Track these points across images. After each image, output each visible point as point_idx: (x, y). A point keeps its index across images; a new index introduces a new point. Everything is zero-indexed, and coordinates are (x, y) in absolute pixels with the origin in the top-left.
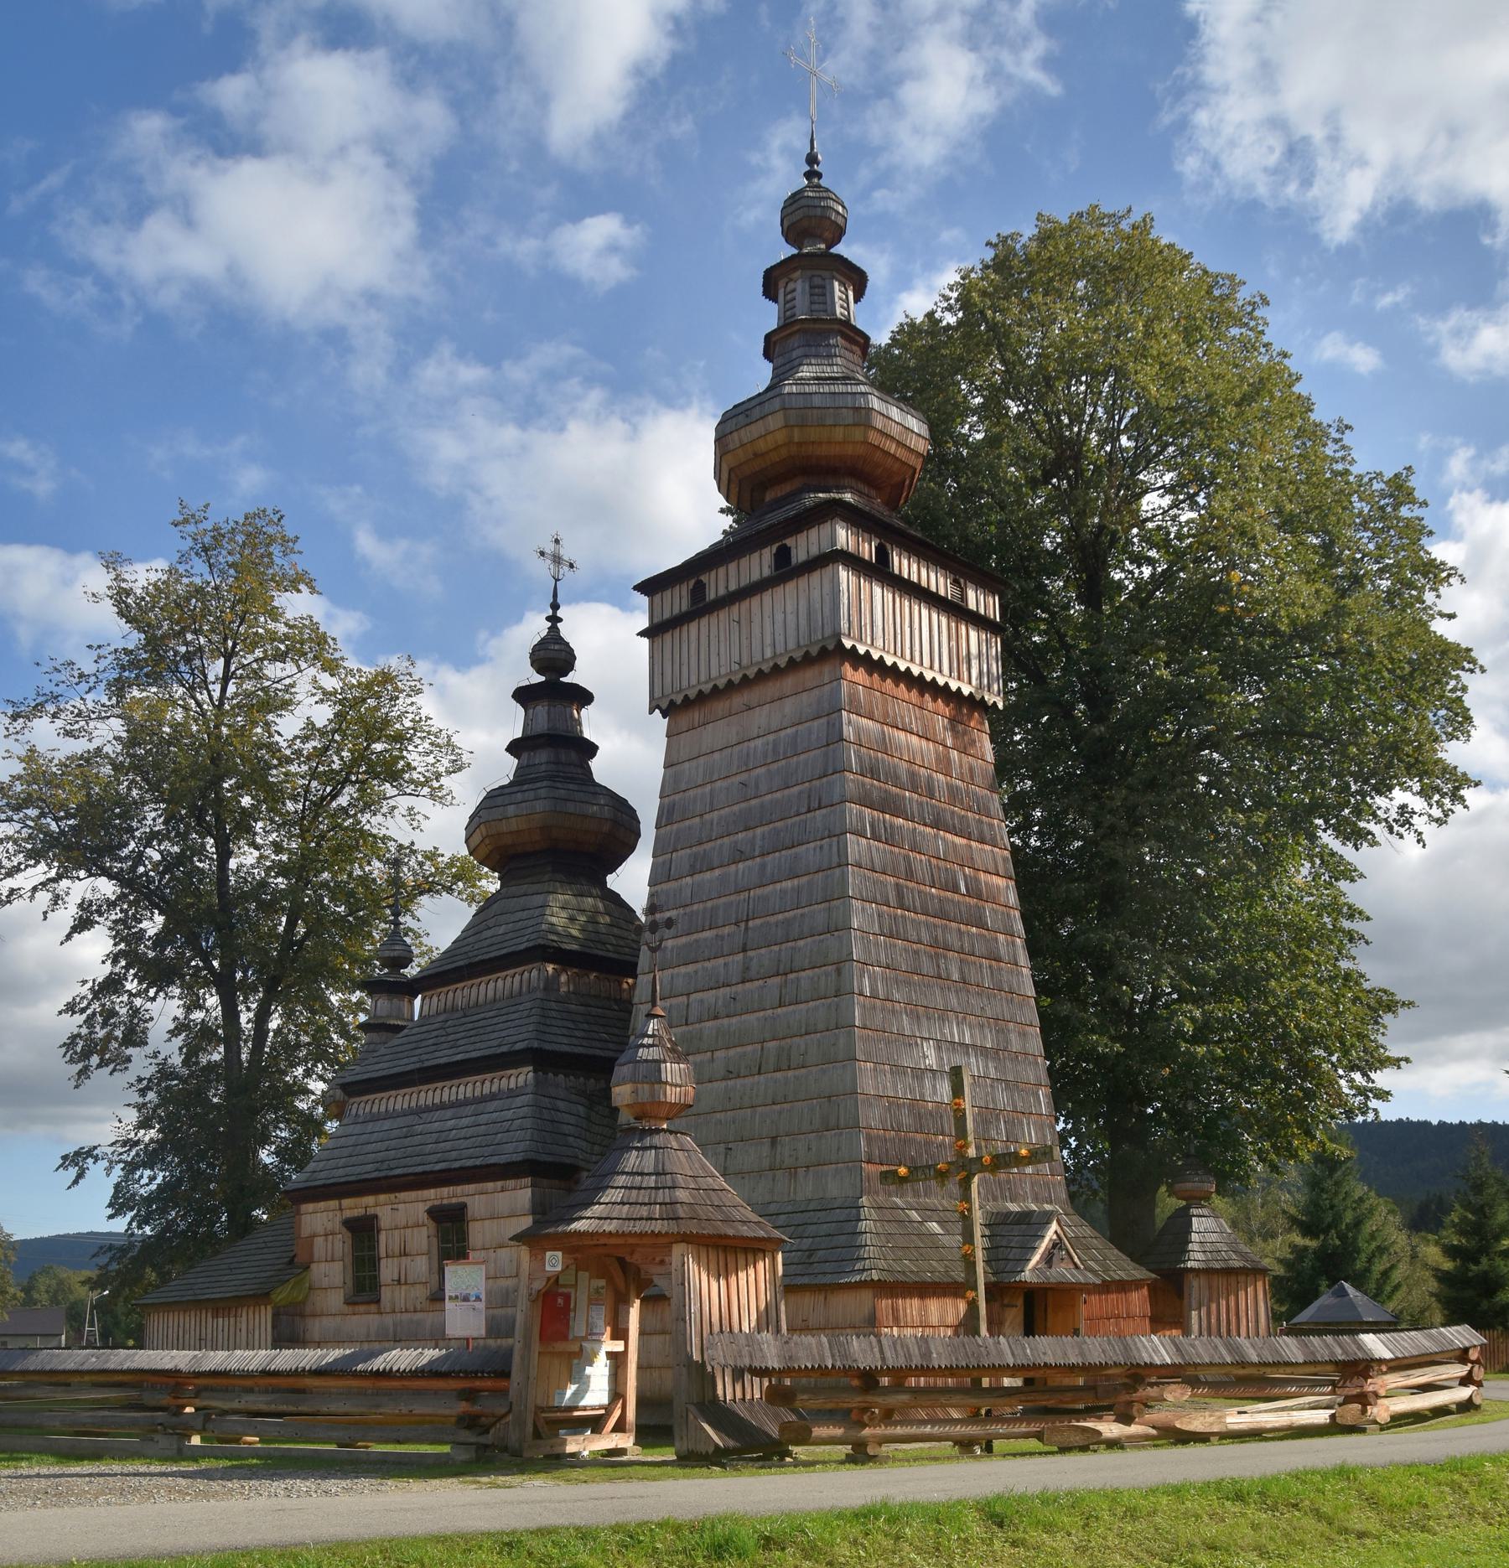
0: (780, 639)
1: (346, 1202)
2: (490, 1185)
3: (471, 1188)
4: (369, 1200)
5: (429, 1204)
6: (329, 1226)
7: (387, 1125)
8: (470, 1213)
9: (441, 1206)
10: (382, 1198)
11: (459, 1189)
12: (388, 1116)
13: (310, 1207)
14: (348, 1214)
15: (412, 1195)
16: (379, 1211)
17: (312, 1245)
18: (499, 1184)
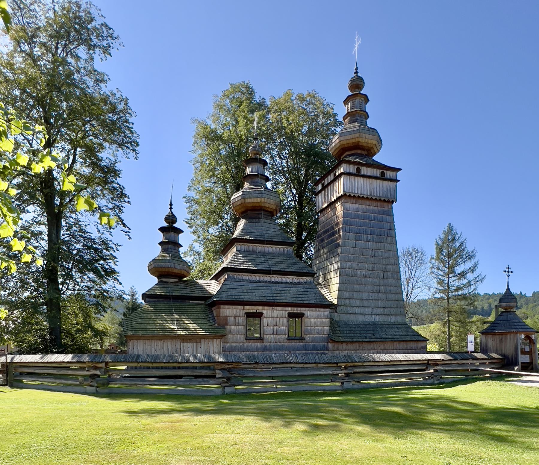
0: (381, 193)
1: (245, 307)
2: (314, 309)
3: (307, 309)
4: (261, 308)
5: (287, 312)
6: (238, 314)
7: (254, 284)
8: (306, 315)
9: (293, 313)
10: (266, 308)
11: (302, 309)
12: (251, 281)
13: (227, 307)
14: (247, 311)
15: (281, 308)
16: (263, 311)
17: (226, 320)
18: (317, 309)
